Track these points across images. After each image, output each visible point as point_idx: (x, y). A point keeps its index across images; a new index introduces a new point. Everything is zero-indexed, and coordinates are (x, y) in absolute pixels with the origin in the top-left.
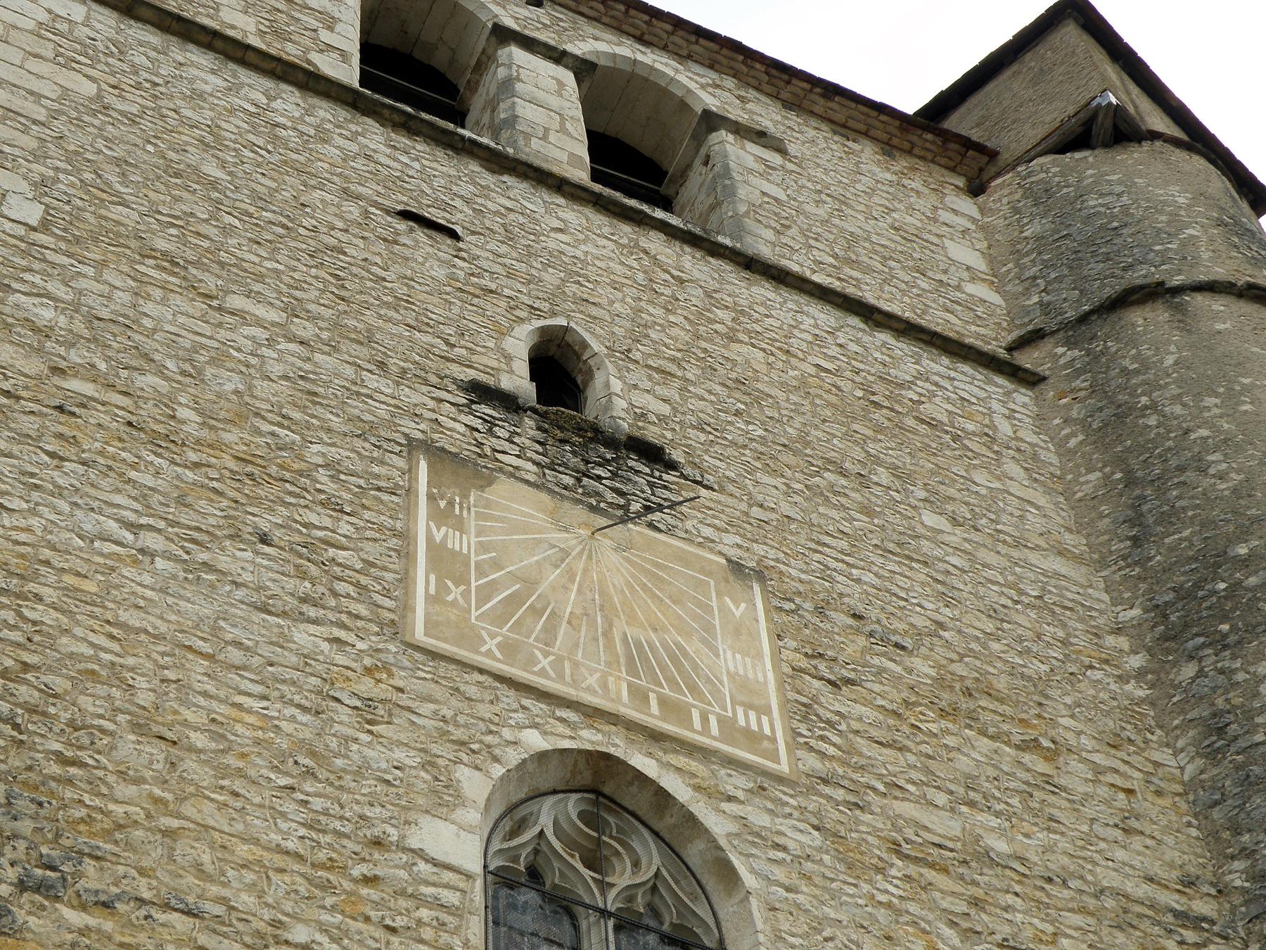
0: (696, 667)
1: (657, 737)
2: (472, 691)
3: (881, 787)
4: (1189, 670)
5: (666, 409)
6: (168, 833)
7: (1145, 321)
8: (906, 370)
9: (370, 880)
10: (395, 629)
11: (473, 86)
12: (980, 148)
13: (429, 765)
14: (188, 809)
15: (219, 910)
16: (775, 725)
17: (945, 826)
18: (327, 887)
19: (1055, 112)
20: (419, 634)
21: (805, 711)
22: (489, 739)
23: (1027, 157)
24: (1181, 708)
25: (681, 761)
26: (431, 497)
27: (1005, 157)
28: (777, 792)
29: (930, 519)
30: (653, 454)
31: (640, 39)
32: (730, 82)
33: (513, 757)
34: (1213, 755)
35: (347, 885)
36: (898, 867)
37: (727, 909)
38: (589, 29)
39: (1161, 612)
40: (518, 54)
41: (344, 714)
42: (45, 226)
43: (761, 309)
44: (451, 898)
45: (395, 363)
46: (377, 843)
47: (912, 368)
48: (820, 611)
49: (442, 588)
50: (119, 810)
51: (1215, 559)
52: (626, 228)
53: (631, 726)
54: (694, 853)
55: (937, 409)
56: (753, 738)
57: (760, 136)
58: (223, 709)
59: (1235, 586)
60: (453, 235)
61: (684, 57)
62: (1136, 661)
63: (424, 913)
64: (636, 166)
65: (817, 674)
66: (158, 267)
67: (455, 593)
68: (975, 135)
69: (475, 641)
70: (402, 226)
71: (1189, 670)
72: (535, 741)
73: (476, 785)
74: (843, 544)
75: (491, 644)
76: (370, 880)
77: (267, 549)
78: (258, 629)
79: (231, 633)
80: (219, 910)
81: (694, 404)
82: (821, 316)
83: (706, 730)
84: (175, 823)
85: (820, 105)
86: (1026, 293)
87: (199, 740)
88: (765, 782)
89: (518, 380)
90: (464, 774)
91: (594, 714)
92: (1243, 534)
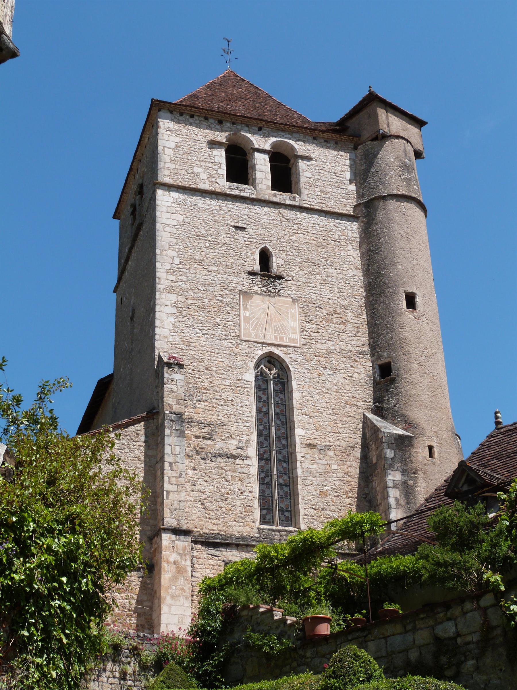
0: (285, 328)
2: (251, 346)
3: (314, 343)
4: (371, 299)
5: (283, 262)
6: (212, 387)
9: (238, 387)
10: (239, 337)
14: (214, 382)
15: (219, 397)
18: (232, 389)
20: (243, 338)
22: (253, 355)
26: (243, 305)
33: (257, 357)
34: (372, 318)
35: (235, 388)
43: (303, 221)
44: (249, 386)
46: (239, 380)
47: (333, 224)
49: (246, 326)
50: (205, 384)
58: (216, 362)
63: (246, 390)
66: (198, 265)
67: (248, 325)
69: (250, 336)
72: (260, 353)
73: (252, 364)
74: (313, 285)
75: (253, 335)
76: (238, 387)
77: (220, 327)
80: (219, 397)
83: (286, 342)
84: (213, 385)
87: (214, 369)
91: (269, 344)
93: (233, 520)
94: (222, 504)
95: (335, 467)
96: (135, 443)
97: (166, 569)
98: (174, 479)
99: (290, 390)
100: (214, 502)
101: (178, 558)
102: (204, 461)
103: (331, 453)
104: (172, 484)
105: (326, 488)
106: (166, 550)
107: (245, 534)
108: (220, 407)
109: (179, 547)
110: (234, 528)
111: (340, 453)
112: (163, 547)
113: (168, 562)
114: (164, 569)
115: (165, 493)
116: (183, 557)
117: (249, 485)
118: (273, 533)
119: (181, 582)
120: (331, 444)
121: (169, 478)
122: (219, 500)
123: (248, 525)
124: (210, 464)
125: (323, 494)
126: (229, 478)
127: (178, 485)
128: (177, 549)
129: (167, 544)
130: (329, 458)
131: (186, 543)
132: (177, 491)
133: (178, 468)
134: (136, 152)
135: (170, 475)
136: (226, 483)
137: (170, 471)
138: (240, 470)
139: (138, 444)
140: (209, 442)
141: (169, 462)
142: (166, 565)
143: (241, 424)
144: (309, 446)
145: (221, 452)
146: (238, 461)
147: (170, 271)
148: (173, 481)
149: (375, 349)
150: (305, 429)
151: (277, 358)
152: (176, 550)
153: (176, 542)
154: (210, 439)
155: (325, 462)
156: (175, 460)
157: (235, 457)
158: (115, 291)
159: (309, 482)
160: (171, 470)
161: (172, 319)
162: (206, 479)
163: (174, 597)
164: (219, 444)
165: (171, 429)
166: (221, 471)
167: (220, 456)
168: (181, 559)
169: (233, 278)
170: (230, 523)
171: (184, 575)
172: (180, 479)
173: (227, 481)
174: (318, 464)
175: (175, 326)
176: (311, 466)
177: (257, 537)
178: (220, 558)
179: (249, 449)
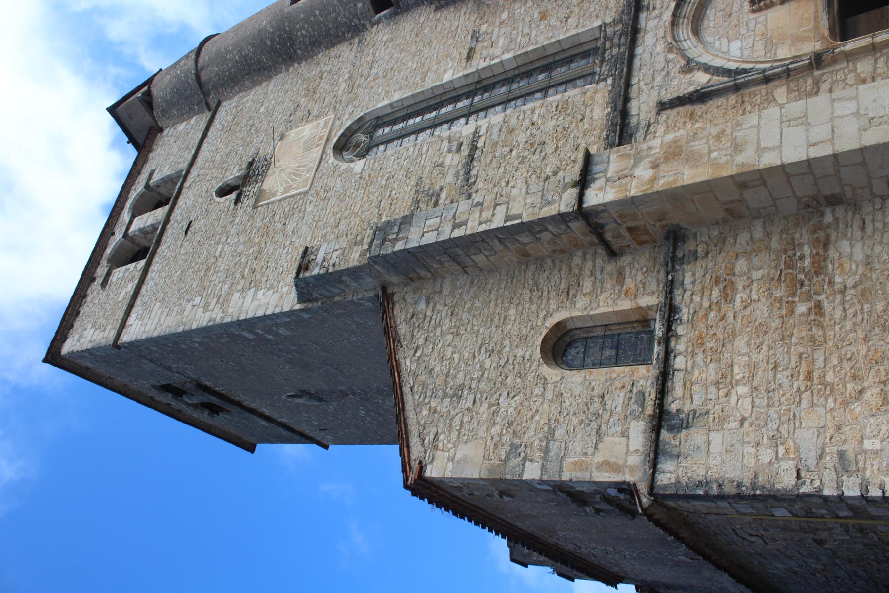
1: (328, 140)
7: (204, 77)
8: (219, 127)
10: (306, 193)
11: (138, 245)
12: (150, 130)
13: (340, 176)
16: (322, 121)
17: (343, 86)
19: (142, 111)
21: (317, 117)
23: (153, 117)
24: (308, 53)
25: (333, 134)
27: (153, 124)
28: (338, 115)
29: (262, 110)
30: (251, 164)
31: (122, 209)
32: (134, 187)
34: (320, 44)
36: (355, 91)
37: (368, 118)
38: (121, 219)
39: (284, 60)
40: (132, 229)
41: (329, 194)
42: (201, 296)
45: (231, 219)
48: (290, 122)
51: (272, 49)
52: (183, 191)
53: (326, 145)
54: (355, 127)
55: (230, 118)
56: (326, 123)
57: (151, 175)
59: (279, 43)
60: (190, 222)
61: (127, 198)
62: (296, 65)
64: (161, 196)
65: (308, 116)
68: (145, 134)
70: (189, 233)
71: (299, 52)
72: (332, 159)
73: (344, 166)
78: (308, 219)
79: (310, 221)
81: (235, 161)
82: (205, 146)
85: (139, 167)
86: (194, 110)
87: (339, 216)
88: (337, 118)
89: (233, 196)
90: (342, 169)
91: (323, 152)
92: (265, 43)
93: (580, 124)
94: (549, 149)
95: (504, 16)
96: (428, 319)
97: (671, 179)
98: (484, 215)
99: (389, 110)
100: (546, 161)
101: (646, 162)
102: (474, 195)
103: (484, 28)
104: (493, 215)
105: (536, 15)
106: (626, 190)
107: (607, 99)
108: (393, 193)
109: (621, 168)
110: (595, 117)
111: (486, 18)
112: (620, 196)
113: (654, 179)
114: (670, 183)
115: (508, 224)
116: (643, 154)
117: (521, 117)
118: (607, 59)
119: (700, 146)
120: (471, 32)
121: (480, 223)
122: (543, 154)
123: (592, 99)
124: (480, 184)
125: (544, 16)
126: (507, 149)
127: (496, 205)
128: (625, 169)
129: (614, 190)
130: (491, 28)
131: (613, 157)
132: (508, 203)
133: (464, 213)
134: (139, 402)
135: (477, 223)
136: (514, 153)
137: (470, 224)
138: (495, 137)
139: (429, 313)
140: (443, 195)
141: (452, 231)
142: (661, 182)
143: (424, 157)
144: (469, 57)
145: (462, 173)
146: (480, 144)
147: (206, 308)
148: (486, 215)
149: (356, 25)
150: (445, 71)
151: (344, 140)
152: (626, 172)
153: (609, 175)
154: (438, 195)
155: (496, 29)
156: (450, 221)
157: (474, 148)
158: (326, 447)
159: (524, 39)
160: (465, 223)
161: (260, 293)
162: (504, 184)
163: (738, 148)
164: (450, 178)
165: (397, 239)
166: (494, 164)
167: (468, 173)
168: (648, 156)
169: (237, 220)
170: (587, 126)
171: (683, 143)
172: (485, 204)
173: (511, 151)
174: (498, 36)
175: (271, 287)
176: (500, 44)
177: (614, 79)
178: (652, 121)
179: (464, 134)
